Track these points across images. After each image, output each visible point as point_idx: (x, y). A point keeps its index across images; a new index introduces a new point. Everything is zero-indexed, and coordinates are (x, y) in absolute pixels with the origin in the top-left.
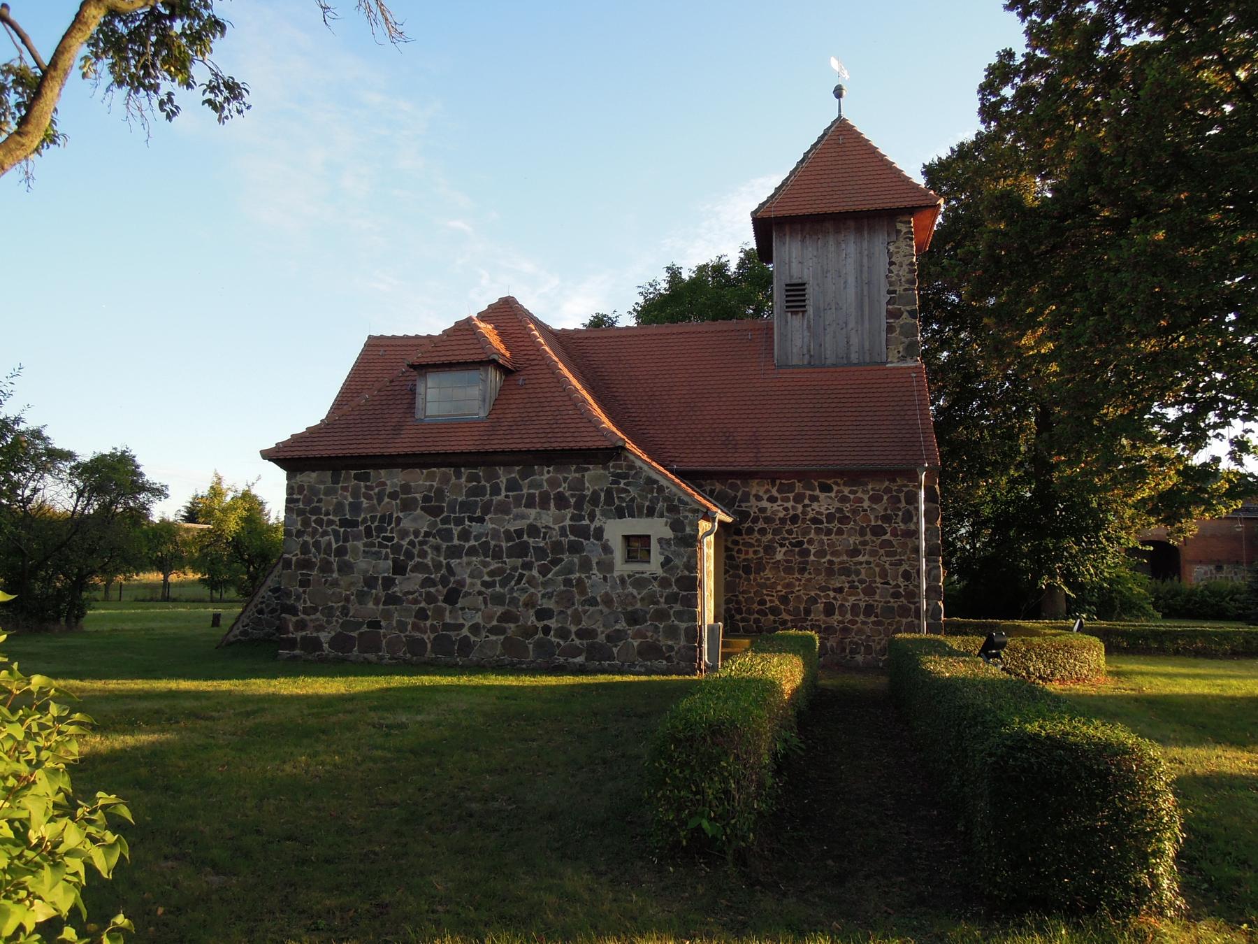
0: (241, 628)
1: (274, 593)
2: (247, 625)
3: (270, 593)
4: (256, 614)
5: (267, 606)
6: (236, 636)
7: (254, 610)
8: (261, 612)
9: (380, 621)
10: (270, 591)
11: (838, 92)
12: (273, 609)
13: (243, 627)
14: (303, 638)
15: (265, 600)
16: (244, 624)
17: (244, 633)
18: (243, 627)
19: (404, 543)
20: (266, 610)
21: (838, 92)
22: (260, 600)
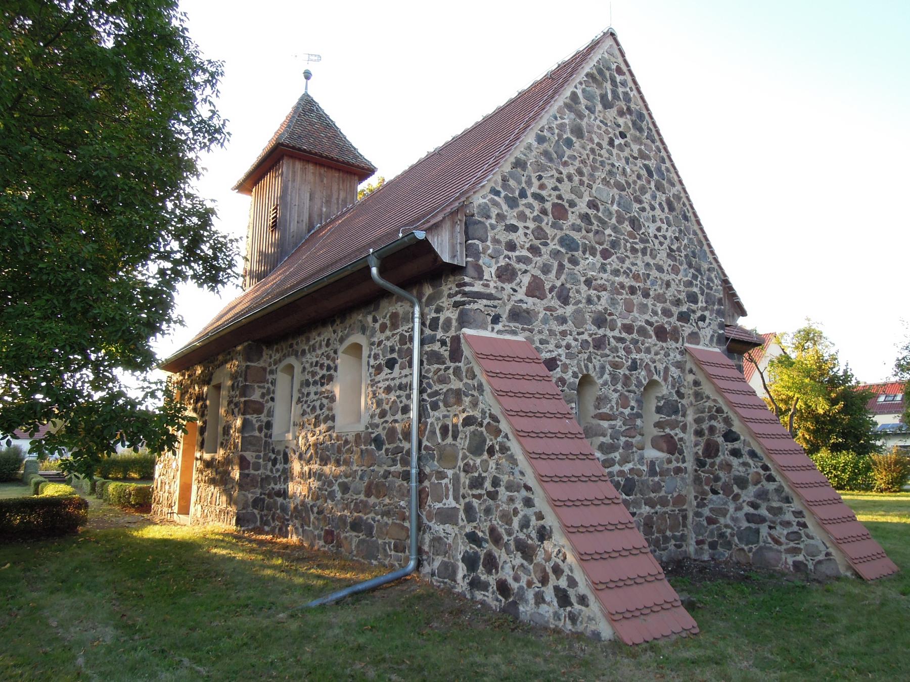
11: (307, 75)
21: (307, 75)
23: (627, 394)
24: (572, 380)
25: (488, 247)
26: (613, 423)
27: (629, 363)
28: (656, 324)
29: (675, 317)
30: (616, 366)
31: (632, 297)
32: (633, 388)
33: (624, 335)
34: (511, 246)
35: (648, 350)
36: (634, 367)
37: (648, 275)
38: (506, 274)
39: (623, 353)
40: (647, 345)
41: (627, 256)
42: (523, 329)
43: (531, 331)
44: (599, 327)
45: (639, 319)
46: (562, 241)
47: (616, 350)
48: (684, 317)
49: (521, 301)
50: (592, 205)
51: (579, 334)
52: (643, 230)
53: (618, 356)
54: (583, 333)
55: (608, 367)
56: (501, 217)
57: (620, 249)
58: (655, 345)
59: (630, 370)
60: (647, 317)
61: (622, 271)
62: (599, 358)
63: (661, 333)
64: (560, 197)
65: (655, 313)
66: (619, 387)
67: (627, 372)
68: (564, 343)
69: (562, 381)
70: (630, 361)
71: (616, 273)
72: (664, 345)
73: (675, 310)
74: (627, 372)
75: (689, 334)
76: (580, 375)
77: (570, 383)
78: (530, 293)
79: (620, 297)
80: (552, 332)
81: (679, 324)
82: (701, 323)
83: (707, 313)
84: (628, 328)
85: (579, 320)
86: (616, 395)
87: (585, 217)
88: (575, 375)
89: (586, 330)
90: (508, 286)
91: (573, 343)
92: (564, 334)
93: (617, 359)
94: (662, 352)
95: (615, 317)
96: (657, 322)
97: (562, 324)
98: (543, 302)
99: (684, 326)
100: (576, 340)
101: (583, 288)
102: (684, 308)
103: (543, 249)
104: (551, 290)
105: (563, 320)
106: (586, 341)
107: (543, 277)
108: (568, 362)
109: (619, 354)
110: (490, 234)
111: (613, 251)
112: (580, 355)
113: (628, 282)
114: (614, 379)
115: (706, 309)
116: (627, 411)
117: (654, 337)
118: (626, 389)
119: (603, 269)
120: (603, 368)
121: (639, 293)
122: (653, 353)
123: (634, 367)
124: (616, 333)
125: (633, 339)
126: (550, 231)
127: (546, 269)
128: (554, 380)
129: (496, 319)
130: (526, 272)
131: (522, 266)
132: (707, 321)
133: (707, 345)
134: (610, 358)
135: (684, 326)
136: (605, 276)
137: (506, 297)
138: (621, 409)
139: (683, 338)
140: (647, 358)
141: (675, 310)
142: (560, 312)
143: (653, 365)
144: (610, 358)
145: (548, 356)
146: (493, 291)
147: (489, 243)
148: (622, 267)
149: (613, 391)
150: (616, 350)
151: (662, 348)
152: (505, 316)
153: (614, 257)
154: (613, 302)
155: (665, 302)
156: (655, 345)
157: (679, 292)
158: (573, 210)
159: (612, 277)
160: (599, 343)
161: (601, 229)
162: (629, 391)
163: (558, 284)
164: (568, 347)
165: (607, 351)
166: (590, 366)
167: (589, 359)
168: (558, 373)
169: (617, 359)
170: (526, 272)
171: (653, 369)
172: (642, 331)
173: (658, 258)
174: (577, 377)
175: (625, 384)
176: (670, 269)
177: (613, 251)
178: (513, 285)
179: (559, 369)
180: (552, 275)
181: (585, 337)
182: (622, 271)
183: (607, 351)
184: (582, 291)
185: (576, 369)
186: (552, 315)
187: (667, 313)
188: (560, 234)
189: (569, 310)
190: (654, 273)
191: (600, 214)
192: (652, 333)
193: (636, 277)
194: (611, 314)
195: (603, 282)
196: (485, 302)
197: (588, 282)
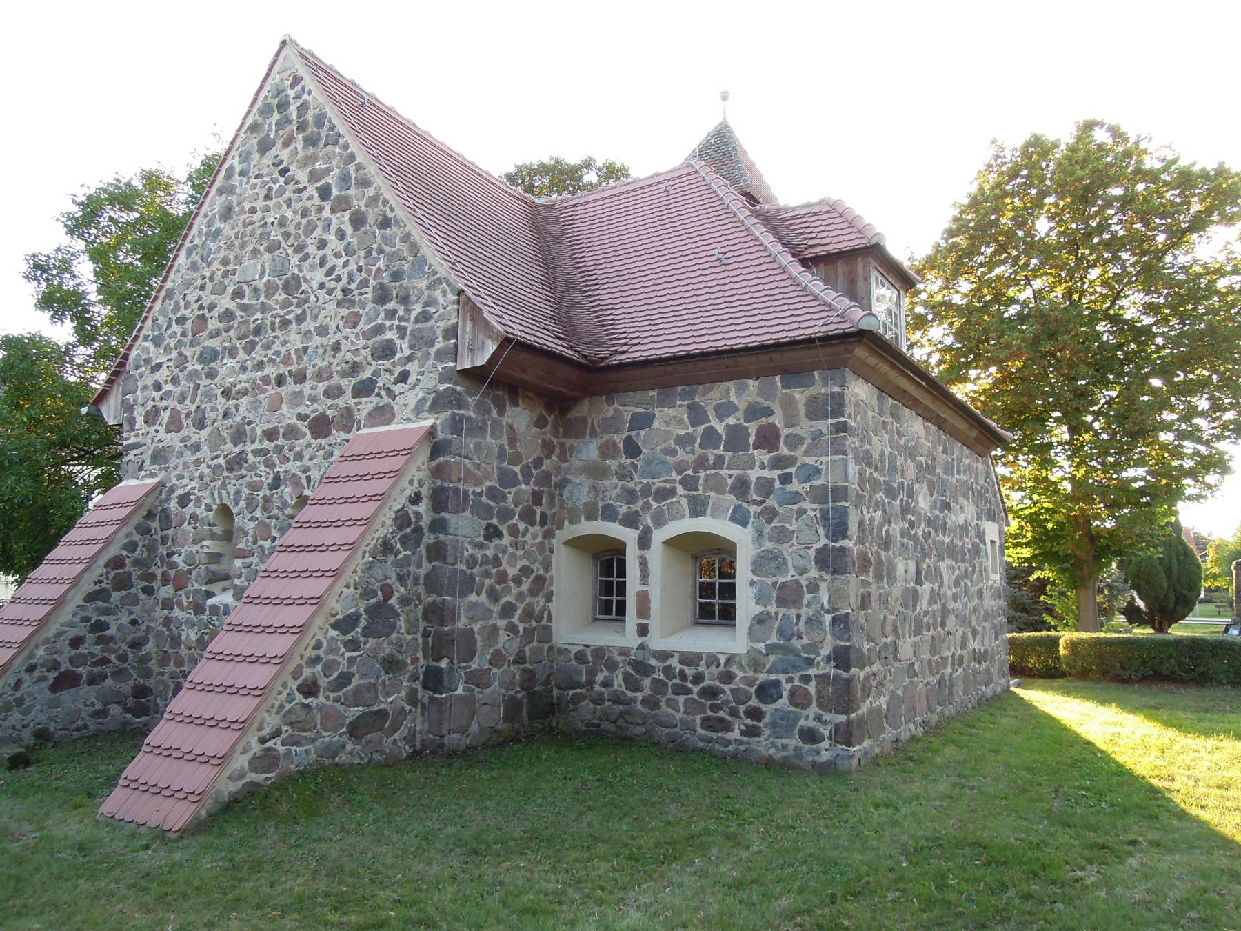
0: (256, 748)
1: (344, 633)
2: (276, 734)
3: (334, 633)
4: (299, 698)
5: (329, 667)
6: (242, 775)
7: (294, 685)
8: (309, 689)
9: (913, 664)
10: (335, 626)
11: (725, 97)
12: (341, 676)
13: (263, 741)
14: (870, 712)
15: (321, 652)
16: (266, 732)
17: (266, 760)
18: (263, 741)
19: (920, 533)
20: (323, 682)
21: (725, 97)
22: (310, 653)
23: (267, 521)
24: (205, 514)
25: (137, 397)
26: (248, 560)
27: (270, 480)
28: (313, 415)
29: (349, 393)
30: (254, 487)
31: (279, 390)
32: (275, 512)
33: (267, 444)
34: (158, 387)
35: (299, 456)
36: (276, 483)
37: (306, 349)
38: (152, 417)
39: (262, 468)
40: (297, 449)
41: (275, 337)
42: (160, 469)
43: (166, 469)
44: (235, 445)
45: (288, 416)
46: (202, 359)
47: (253, 467)
48: (364, 389)
49: (160, 441)
50: (238, 294)
51: (213, 459)
52: (304, 286)
53: (256, 475)
54: (218, 457)
55: (245, 492)
56: (148, 361)
57: (266, 333)
58: (309, 445)
59: (271, 489)
60: (301, 410)
61: (265, 360)
62: (233, 482)
63: (320, 426)
64: (201, 308)
65: (313, 399)
66: (258, 513)
67: (268, 493)
68: (197, 474)
69: (194, 517)
70: (271, 477)
71: (260, 366)
72: (324, 442)
73: (348, 384)
74: (268, 493)
75: (369, 414)
76: (214, 507)
77: (202, 518)
78: (168, 431)
79: (263, 396)
80: (186, 466)
81: (352, 401)
82: (397, 389)
83: (413, 367)
84: (270, 435)
85: (216, 440)
86: (252, 525)
87: (228, 315)
88: (209, 508)
89: (222, 452)
90: (152, 430)
91: (207, 471)
92: (198, 463)
93: (255, 478)
94: (321, 453)
95: (254, 425)
96: (313, 411)
97: (195, 452)
98: (179, 434)
99: (360, 403)
100: (209, 467)
101: (221, 400)
102: (367, 374)
103: (181, 376)
104: (188, 415)
105: (196, 448)
106: (220, 465)
107: (179, 407)
108: (200, 494)
109: (258, 472)
110: (140, 384)
111: (257, 339)
112: (212, 484)
113: (271, 371)
114: (251, 505)
115: (409, 359)
116: (267, 544)
117: (309, 436)
118: (266, 515)
119: (243, 368)
120: (238, 493)
121: (290, 380)
122: (307, 458)
123: (276, 483)
124: (257, 446)
125: (277, 446)
126: (187, 352)
127: (182, 400)
128: (188, 517)
129: (141, 469)
130: (166, 408)
131: (164, 403)
132: (412, 379)
133: (409, 420)
134: (248, 479)
135: (360, 403)
136: (243, 377)
137: (149, 441)
138: (261, 542)
139: (360, 422)
140: (293, 466)
141: (348, 384)
142: (194, 439)
143: (303, 476)
144: (248, 479)
145: (180, 492)
146: (140, 439)
147: (139, 393)
148: (266, 356)
149: (250, 519)
150: (253, 467)
151: (320, 448)
152: (148, 462)
153: (258, 348)
154: (255, 406)
155: (331, 377)
156: (309, 445)
157: (356, 352)
158: (211, 314)
159: (253, 375)
160: (236, 462)
161: (246, 318)
162: (269, 518)
163: (193, 408)
164: (201, 477)
165: (243, 472)
166: (224, 492)
167: (224, 484)
168: (191, 508)
169: (255, 478)
170: (166, 408)
171: (304, 482)
172: (292, 432)
173: (320, 318)
174: (211, 510)
175: (265, 509)
176: (341, 324)
177: (257, 339)
178: (156, 427)
179: (191, 505)
180: (188, 402)
181: (221, 461)
182: (265, 360)
183: (243, 472)
184: (219, 407)
185: (208, 501)
186: (186, 446)
187: (333, 392)
188: (198, 350)
189: (204, 433)
190: (317, 340)
191: (246, 301)
192: (306, 430)
193: (287, 360)
194: (250, 423)
195: (243, 385)
196: (135, 452)
197: (226, 394)
